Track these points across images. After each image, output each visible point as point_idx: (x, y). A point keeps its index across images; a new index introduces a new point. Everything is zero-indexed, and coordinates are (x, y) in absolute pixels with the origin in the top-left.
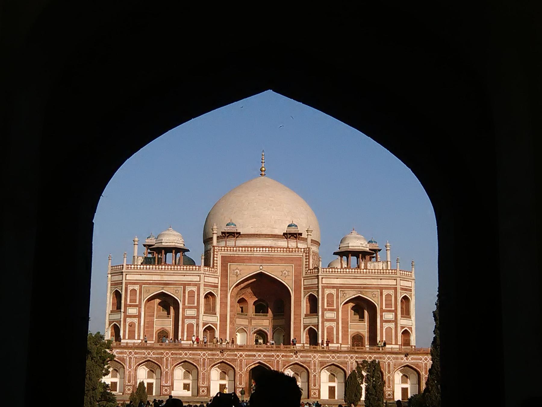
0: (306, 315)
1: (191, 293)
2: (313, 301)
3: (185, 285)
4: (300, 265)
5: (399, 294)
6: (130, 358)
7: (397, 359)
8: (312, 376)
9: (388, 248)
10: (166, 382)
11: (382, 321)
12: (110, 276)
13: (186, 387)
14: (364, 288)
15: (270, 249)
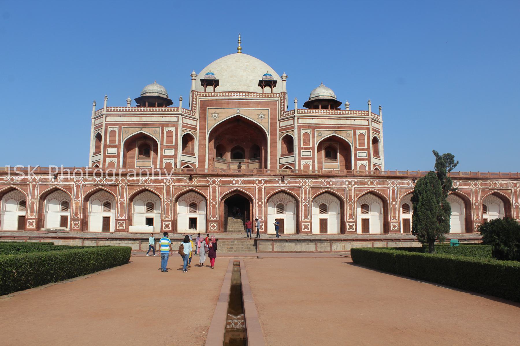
0: (282, 156)
1: (170, 132)
2: (289, 141)
3: (163, 126)
4: (276, 109)
5: (371, 133)
6: (78, 186)
7: (403, 184)
8: (302, 206)
9: (347, 106)
10: (121, 215)
11: (356, 159)
12: (93, 120)
13: (150, 221)
14: (339, 128)
15: (247, 94)
